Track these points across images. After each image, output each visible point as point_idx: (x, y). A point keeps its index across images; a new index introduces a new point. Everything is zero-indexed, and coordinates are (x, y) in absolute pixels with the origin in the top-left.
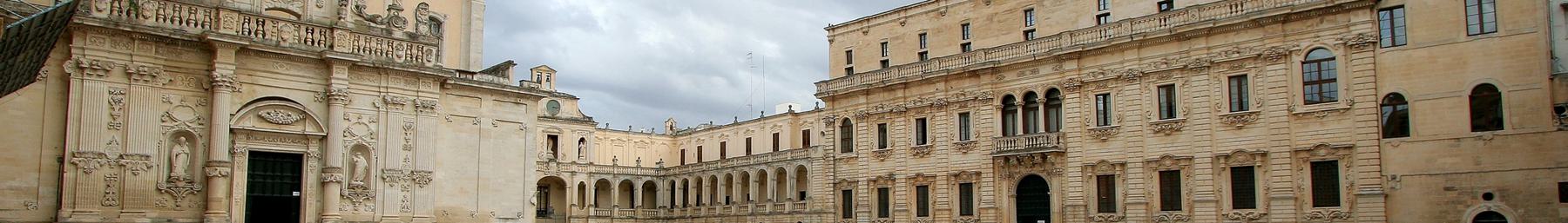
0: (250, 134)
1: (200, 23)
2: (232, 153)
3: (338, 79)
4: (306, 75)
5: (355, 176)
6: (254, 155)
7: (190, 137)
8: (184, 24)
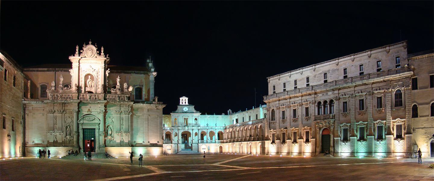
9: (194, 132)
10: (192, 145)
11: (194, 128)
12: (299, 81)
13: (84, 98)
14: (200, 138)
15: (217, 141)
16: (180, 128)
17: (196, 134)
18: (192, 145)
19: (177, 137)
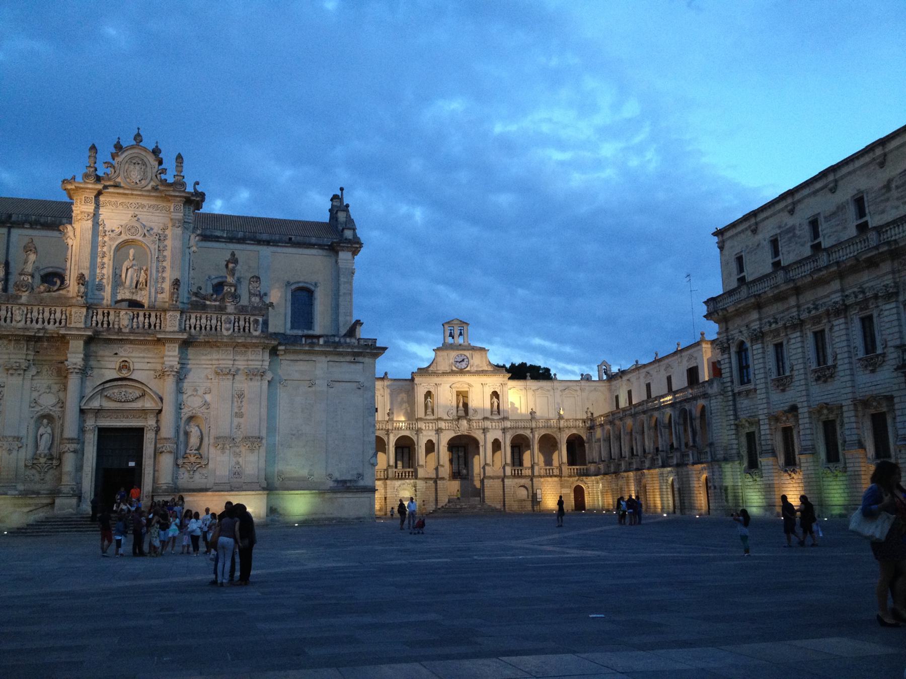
0: (98, 412)
1: (58, 320)
2: (82, 430)
3: (170, 356)
4: (146, 355)
5: (190, 446)
6: (104, 433)
7: (49, 417)
8: (46, 323)
9: (491, 437)
10: (482, 481)
11: (488, 424)
12: (825, 218)
13: (109, 324)
14: (509, 460)
15: (566, 469)
16: (442, 425)
17: (496, 445)
18: (482, 481)
19: (432, 456)
